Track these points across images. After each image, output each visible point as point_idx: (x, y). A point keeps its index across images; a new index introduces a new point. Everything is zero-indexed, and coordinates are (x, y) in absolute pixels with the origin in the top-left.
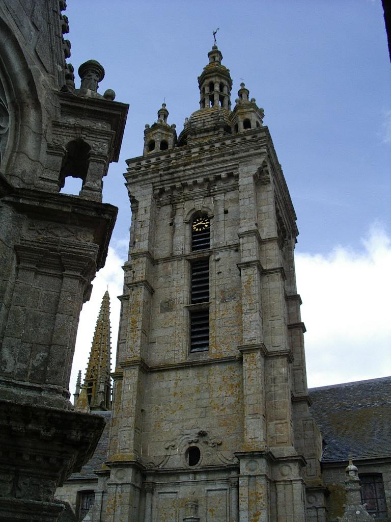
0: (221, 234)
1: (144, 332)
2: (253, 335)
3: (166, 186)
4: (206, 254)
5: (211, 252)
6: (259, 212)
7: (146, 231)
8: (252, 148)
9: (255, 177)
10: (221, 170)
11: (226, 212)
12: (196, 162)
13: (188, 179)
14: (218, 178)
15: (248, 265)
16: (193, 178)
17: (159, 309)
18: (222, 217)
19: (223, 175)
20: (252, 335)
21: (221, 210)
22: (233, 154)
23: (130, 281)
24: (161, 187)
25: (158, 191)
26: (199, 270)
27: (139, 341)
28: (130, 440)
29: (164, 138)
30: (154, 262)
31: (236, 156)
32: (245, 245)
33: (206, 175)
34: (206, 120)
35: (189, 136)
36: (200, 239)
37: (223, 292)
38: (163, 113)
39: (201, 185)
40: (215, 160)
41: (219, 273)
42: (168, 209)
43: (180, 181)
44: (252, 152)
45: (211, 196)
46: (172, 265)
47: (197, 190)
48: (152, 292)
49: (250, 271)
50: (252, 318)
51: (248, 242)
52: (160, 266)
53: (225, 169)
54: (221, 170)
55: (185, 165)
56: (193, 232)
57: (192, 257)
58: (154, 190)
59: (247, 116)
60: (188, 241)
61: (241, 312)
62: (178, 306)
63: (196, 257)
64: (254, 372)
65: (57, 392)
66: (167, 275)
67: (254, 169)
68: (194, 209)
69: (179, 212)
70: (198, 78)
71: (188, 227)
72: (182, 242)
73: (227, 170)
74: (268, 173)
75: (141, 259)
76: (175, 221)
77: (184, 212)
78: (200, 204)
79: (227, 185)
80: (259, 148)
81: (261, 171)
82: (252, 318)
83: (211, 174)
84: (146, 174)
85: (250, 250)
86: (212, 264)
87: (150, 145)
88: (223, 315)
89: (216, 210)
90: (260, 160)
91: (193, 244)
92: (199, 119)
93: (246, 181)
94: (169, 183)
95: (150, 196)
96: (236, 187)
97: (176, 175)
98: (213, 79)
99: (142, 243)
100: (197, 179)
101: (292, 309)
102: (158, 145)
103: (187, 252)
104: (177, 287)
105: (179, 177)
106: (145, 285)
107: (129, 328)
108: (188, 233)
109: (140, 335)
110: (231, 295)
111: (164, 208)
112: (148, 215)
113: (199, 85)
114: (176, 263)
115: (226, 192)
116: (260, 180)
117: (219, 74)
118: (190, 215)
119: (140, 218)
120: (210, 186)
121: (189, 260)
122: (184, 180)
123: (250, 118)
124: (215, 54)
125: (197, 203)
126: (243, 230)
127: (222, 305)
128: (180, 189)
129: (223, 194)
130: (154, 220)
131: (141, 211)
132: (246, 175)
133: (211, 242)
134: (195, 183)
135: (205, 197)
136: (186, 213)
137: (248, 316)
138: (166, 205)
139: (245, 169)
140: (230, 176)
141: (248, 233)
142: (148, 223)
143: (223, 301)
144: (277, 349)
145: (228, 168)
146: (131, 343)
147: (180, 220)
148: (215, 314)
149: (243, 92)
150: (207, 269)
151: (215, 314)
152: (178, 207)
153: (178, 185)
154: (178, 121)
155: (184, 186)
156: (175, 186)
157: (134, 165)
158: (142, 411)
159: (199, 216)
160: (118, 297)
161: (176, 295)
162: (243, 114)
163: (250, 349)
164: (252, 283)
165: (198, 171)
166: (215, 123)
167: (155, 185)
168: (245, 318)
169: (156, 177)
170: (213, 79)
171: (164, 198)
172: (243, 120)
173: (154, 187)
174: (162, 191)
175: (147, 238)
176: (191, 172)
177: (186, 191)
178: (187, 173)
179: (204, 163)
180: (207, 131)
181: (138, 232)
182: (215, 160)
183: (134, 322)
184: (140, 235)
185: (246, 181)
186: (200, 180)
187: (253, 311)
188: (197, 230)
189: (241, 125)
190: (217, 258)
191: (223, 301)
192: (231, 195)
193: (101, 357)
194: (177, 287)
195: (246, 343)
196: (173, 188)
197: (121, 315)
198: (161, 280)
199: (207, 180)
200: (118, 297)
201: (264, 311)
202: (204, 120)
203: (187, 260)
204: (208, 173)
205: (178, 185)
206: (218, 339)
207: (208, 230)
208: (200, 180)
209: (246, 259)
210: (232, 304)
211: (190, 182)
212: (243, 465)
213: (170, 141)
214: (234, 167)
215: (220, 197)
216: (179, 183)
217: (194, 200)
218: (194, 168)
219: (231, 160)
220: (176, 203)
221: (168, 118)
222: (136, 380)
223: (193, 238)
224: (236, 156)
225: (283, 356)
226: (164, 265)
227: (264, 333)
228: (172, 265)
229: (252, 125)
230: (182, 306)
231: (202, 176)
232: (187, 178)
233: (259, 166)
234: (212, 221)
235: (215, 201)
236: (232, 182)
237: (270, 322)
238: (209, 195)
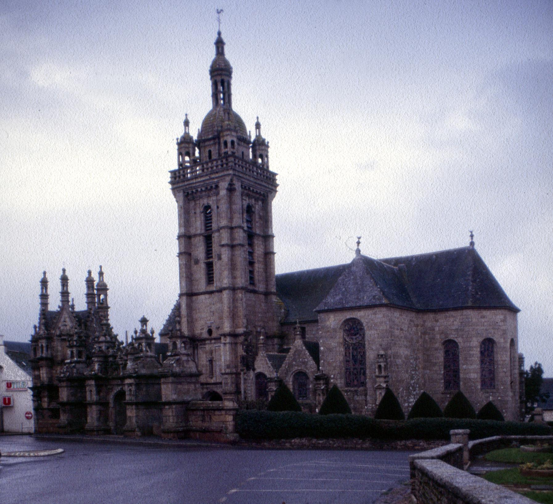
19: (214, 186)
39: (205, 191)
47: (204, 193)
58: (184, 192)
60: (203, 224)
81: (231, 184)
93: (223, 192)
108: (203, 218)
116: (231, 189)
128: (195, 193)
147: (198, 211)
155: (197, 191)
159: (207, 207)
171: (190, 197)
177: (199, 194)
199: (207, 188)
205: (194, 191)
208: (203, 189)
211: (199, 189)
212: (222, 338)
219: (217, 178)
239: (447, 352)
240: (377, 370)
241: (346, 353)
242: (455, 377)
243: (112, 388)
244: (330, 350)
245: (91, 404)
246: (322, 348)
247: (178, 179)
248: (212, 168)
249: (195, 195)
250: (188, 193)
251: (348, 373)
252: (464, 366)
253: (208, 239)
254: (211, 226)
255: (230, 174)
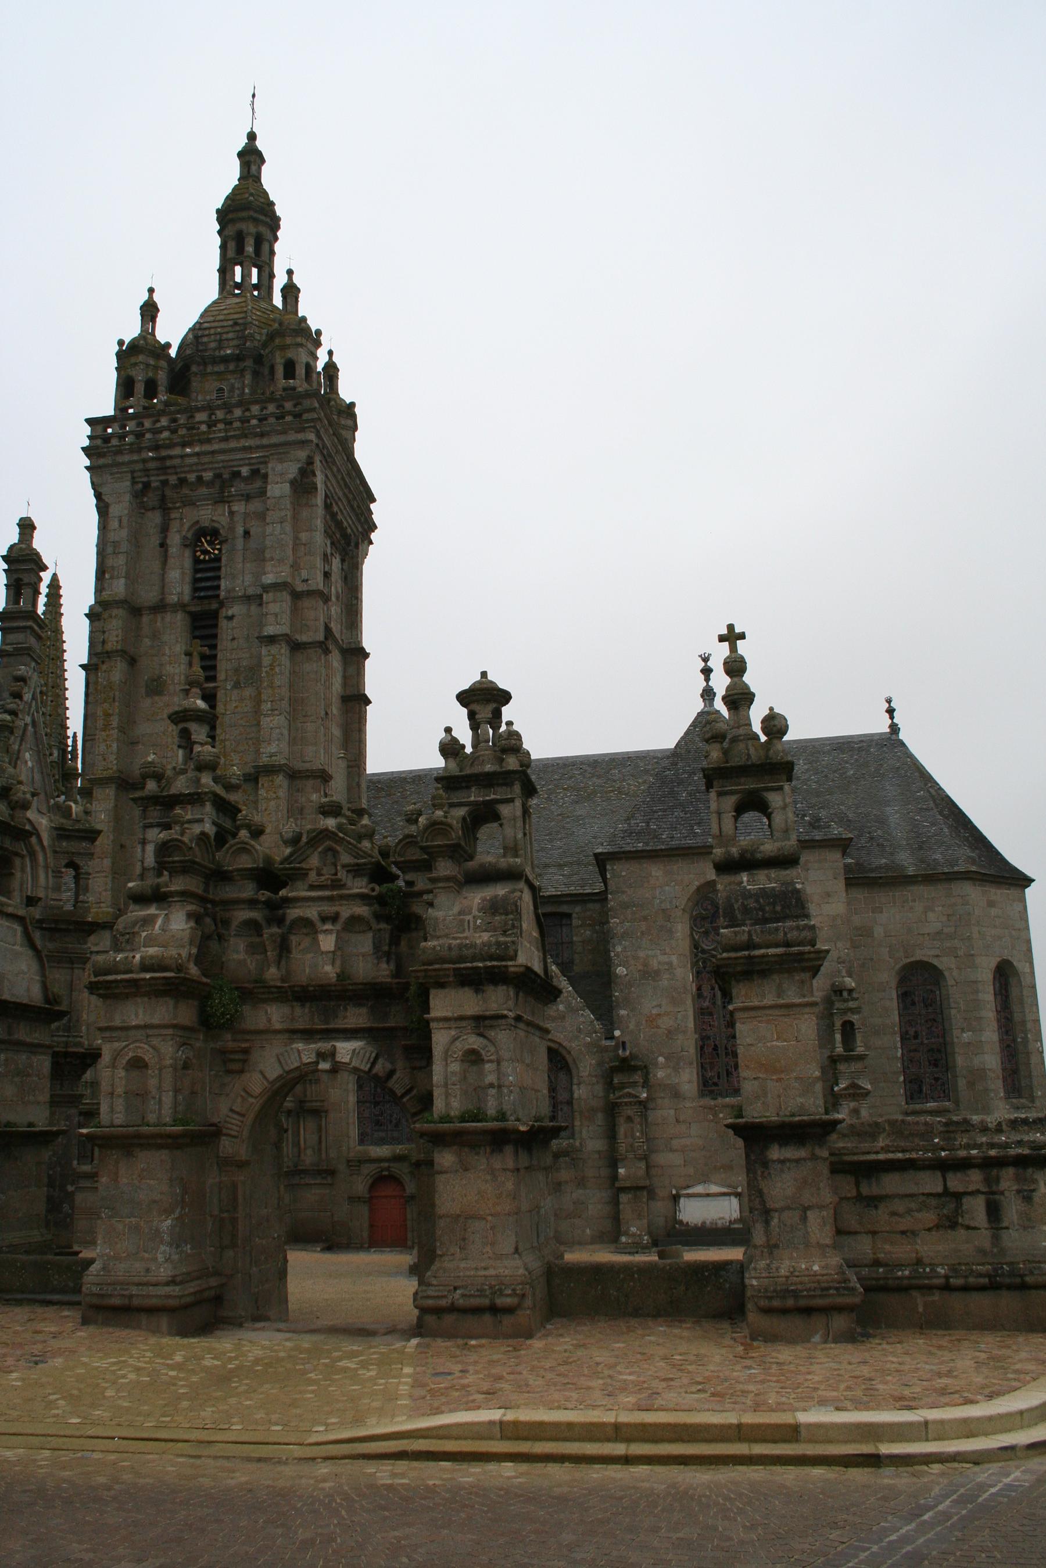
0: (237, 578)
1: (122, 730)
2: (275, 749)
3: (152, 478)
4: (214, 606)
5: (222, 604)
6: (297, 543)
7: (121, 560)
8: (292, 429)
9: (293, 483)
10: (241, 463)
11: (247, 533)
12: (202, 442)
13: (189, 472)
14: (237, 475)
15: (272, 640)
16: (198, 471)
17: (143, 690)
18: (240, 543)
19: (245, 471)
20: (273, 748)
21: (240, 530)
22: (262, 435)
23: (99, 649)
24: (145, 479)
25: (140, 486)
26: (204, 624)
27: (115, 745)
28: (106, 890)
29: (150, 374)
30: (135, 611)
31: (265, 441)
32: (271, 605)
33: (216, 468)
34: (225, 336)
35: (194, 368)
36: (206, 574)
37: (236, 670)
38: (149, 311)
39: (210, 484)
40: (233, 444)
41: (233, 639)
42: (155, 518)
43: (176, 473)
44: (293, 436)
45: (224, 502)
46: (163, 619)
47: (204, 491)
48: (132, 661)
49: (274, 649)
50: (274, 723)
51: (275, 601)
52: (145, 619)
53: (247, 462)
54: (241, 463)
55: (184, 445)
56: (197, 561)
57: (193, 609)
58: (134, 482)
59: (290, 354)
60: (188, 579)
61: (257, 712)
62: (171, 688)
63: (198, 608)
64: (272, 803)
65: (77, 1036)
66: (155, 636)
67: (292, 470)
68: (198, 522)
69: (175, 526)
70: (218, 211)
71: (188, 553)
72: (178, 582)
73: (250, 464)
74: (314, 475)
75: (115, 612)
76: (168, 541)
77: (182, 525)
78: (207, 514)
79: (249, 487)
80: (302, 430)
81: (306, 472)
82: (274, 723)
83: (224, 467)
84: (119, 452)
85: (276, 615)
86: (223, 623)
87: (125, 387)
88: (236, 707)
89: (232, 529)
90: (302, 454)
91: (196, 580)
92: (212, 331)
93: (278, 489)
94: (158, 475)
95: (127, 497)
96: (262, 493)
97: (168, 463)
98: (242, 226)
99: (115, 582)
100: (204, 474)
101: (351, 670)
102: (140, 388)
103: (187, 598)
104: (170, 656)
105: (174, 467)
106: (121, 656)
107: (100, 723)
108: (188, 563)
109: (115, 736)
110: (250, 675)
111: (150, 514)
112: (124, 533)
113: (218, 227)
114: (168, 617)
115: (248, 498)
116: (303, 486)
117: (255, 215)
118: (191, 532)
119: (112, 536)
120: (223, 486)
121: (190, 613)
122: (182, 472)
123: (295, 358)
124: (252, 136)
125: (202, 512)
126: (269, 579)
127: (236, 692)
128: (175, 486)
129: (243, 503)
130: (136, 538)
131: (114, 524)
132: (281, 474)
133: (223, 584)
134: (200, 479)
135: (216, 502)
136: (186, 527)
137: (268, 719)
138: (153, 509)
139: (279, 467)
140: (255, 473)
141: (276, 587)
142: (124, 547)
143: (237, 685)
144: (307, 766)
145: (253, 461)
146: (102, 747)
147: (175, 540)
148: (225, 705)
149: (291, 291)
150: (216, 626)
151: (225, 705)
152: (173, 516)
153: (173, 479)
154: (172, 331)
155: (183, 481)
156: (167, 480)
157: (99, 428)
158: (122, 846)
160: (81, 666)
161: (169, 669)
162: (284, 348)
163: (271, 770)
164: (277, 670)
165: (206, 459)
166: (238, 346)
167: (136, 475)
168: (265, 721)
169: (136, 462)
170: (242, 226)
171: (151, 499)
172: (283, 361)
173: (133, 478)
174: (147, 486)
175: (123, 574)
176: (195, 460)
177: (185, 491)
178: (189, 461)
179: (216, 447)
180: (225, 360)
181: (110, 562)
182: (233, 444)
183: (107, 715)
184: (113, 568)
185: (278, 489)
186: (208, 475)
187: (276, 712)
188: (202, 557)
189: (280, 371)
190: (230, 613)
191: (237, 685)
192: (255, 505)
193: (50, 699)
194: (170, 656)
195: (264, 760)
196: (165, 483)
197: (87, 695)
198: (147, 642)
199: (218, 476)
200: (81, 666)
201: (296, 709)
202: (220, 334)
203: (185, 611)
204: (221, 465)
206: (227, 743)
207: (218, 559)
208: (208, 475)
209: (270, 630)
210: (248, 692)
211: (192, 477)
213: (162, 377)
214: (262, 460)
215: (239, 507)
216: (175, 477)
217: (198, 506)
218: (198, 454)
219: (258, 447)
220: (169, 509)
221: (158, 319)
222: (112, 805)
223: (196, 571)
224: (265, 441)
225: (316, 777)
226: (152, 616)
227: (292, 741)
228: (163, 619)
229: (297, 372)
230: (178, 688)
231: (211, 469)
232: (186, 469)
233: (299, 466)
234: (225, 547)
235: (232, 513)
236: (258, 484)
237: (300, 725)
238: (221, 500)
239: (905, 997)
240: (838, 1037)
241: (699, 989)
242: (936, 1065)
243: (246, 1051)
244: (649, 974)
245: (127, 1143)
246: (621, 970)
247: (105, 446)
248: (244, 421)
249: (168, 492)
250: (147, 486)
251: (708, 1050)
252: (966, 1036)
253: (204, 624)
254: (218, 587)
255: (304, 443)
